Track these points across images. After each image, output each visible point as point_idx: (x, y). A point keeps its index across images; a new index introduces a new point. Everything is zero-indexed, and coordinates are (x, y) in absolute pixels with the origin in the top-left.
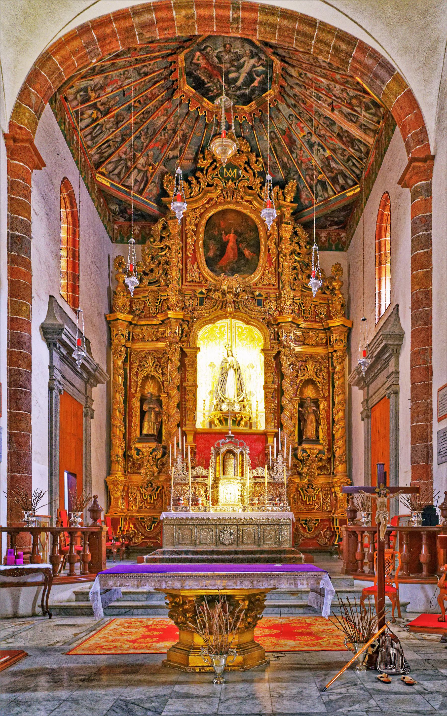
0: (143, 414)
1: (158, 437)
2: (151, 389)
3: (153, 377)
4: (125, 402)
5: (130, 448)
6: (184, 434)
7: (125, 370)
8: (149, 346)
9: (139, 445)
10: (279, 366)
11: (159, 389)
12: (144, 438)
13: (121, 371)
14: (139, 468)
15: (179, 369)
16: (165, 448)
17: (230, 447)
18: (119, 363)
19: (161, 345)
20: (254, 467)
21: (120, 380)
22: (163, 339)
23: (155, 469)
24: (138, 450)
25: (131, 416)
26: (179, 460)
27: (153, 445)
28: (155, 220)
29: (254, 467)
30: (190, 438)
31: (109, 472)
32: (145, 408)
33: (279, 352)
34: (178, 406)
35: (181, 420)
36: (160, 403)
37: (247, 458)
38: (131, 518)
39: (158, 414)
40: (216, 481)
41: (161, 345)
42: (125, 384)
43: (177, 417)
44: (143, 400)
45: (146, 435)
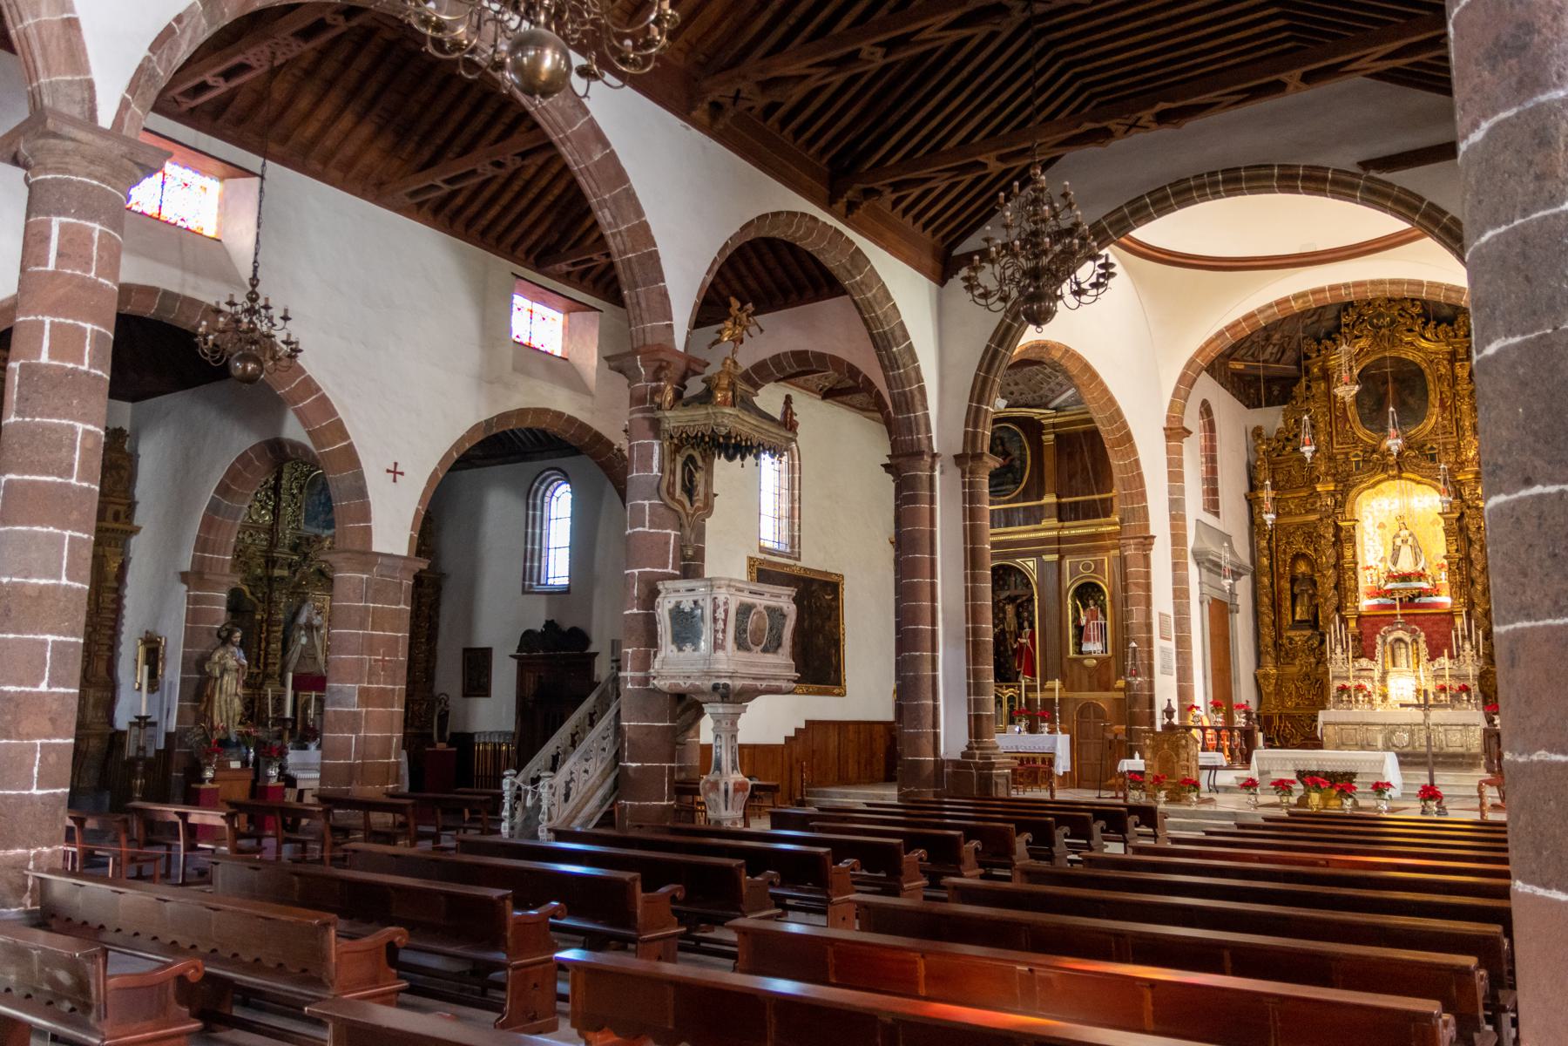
0: (1294, 597)
1: (1313, 623)
2: (1302, 568)
3: (1304, 556)
4: (1272, 585)
5: (1281, 636)
6: (1344, 620)
7: (1270, 548)
8: (1298, 520)
9: (1291, 634)
10: (1463, 530)
11: (1312, 568)
12: (1298, 625)
13: (1266, 552)
14: (1294, 658)
15: (1334, 544)
16: (1323, 635)
17: (1400, 634)
18: (1264, 543)
19: (1313, 517)
20: (1432, 658)
21: (1265, 561)
22: (1314, 511)
23: (1312, 660)
24: (1291, 639)
25: (1280, 599)
26: (1339, 650)
27: (1308, 633)
28: (1297, 380)
29: (1432, 658)
30: (1353, 624)
31: (1259, 665)
32: (1296, 590)
33: (1462, 514)
34: (1336, 587)
35: (1340, 601)
36: (1314, 583)
37: (1422, 645)
38: (1289, 717)
39: (1312, 597)
40: (1385, 674)
41: (1313, 517)
42: (1271, 565)
43: (1335, 601)
44: (1294, 580)
45: (1300, 621)
